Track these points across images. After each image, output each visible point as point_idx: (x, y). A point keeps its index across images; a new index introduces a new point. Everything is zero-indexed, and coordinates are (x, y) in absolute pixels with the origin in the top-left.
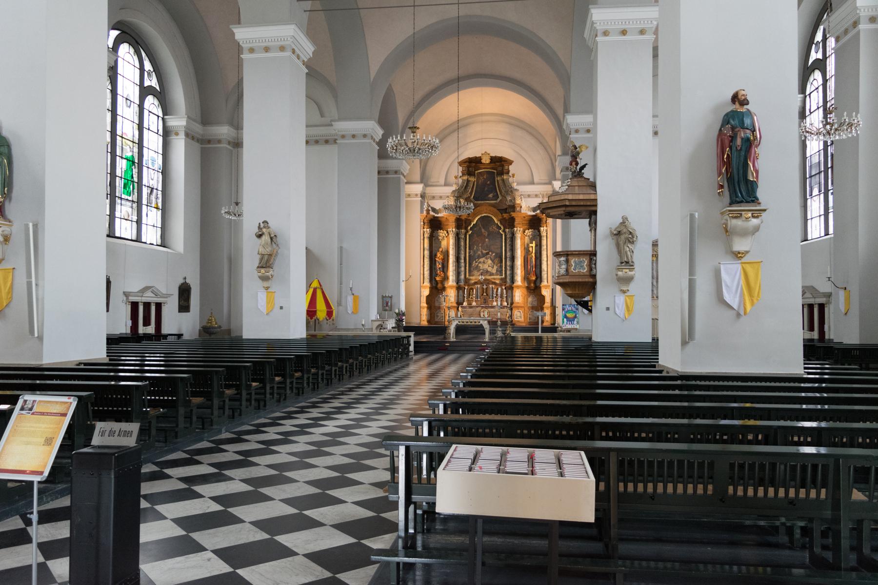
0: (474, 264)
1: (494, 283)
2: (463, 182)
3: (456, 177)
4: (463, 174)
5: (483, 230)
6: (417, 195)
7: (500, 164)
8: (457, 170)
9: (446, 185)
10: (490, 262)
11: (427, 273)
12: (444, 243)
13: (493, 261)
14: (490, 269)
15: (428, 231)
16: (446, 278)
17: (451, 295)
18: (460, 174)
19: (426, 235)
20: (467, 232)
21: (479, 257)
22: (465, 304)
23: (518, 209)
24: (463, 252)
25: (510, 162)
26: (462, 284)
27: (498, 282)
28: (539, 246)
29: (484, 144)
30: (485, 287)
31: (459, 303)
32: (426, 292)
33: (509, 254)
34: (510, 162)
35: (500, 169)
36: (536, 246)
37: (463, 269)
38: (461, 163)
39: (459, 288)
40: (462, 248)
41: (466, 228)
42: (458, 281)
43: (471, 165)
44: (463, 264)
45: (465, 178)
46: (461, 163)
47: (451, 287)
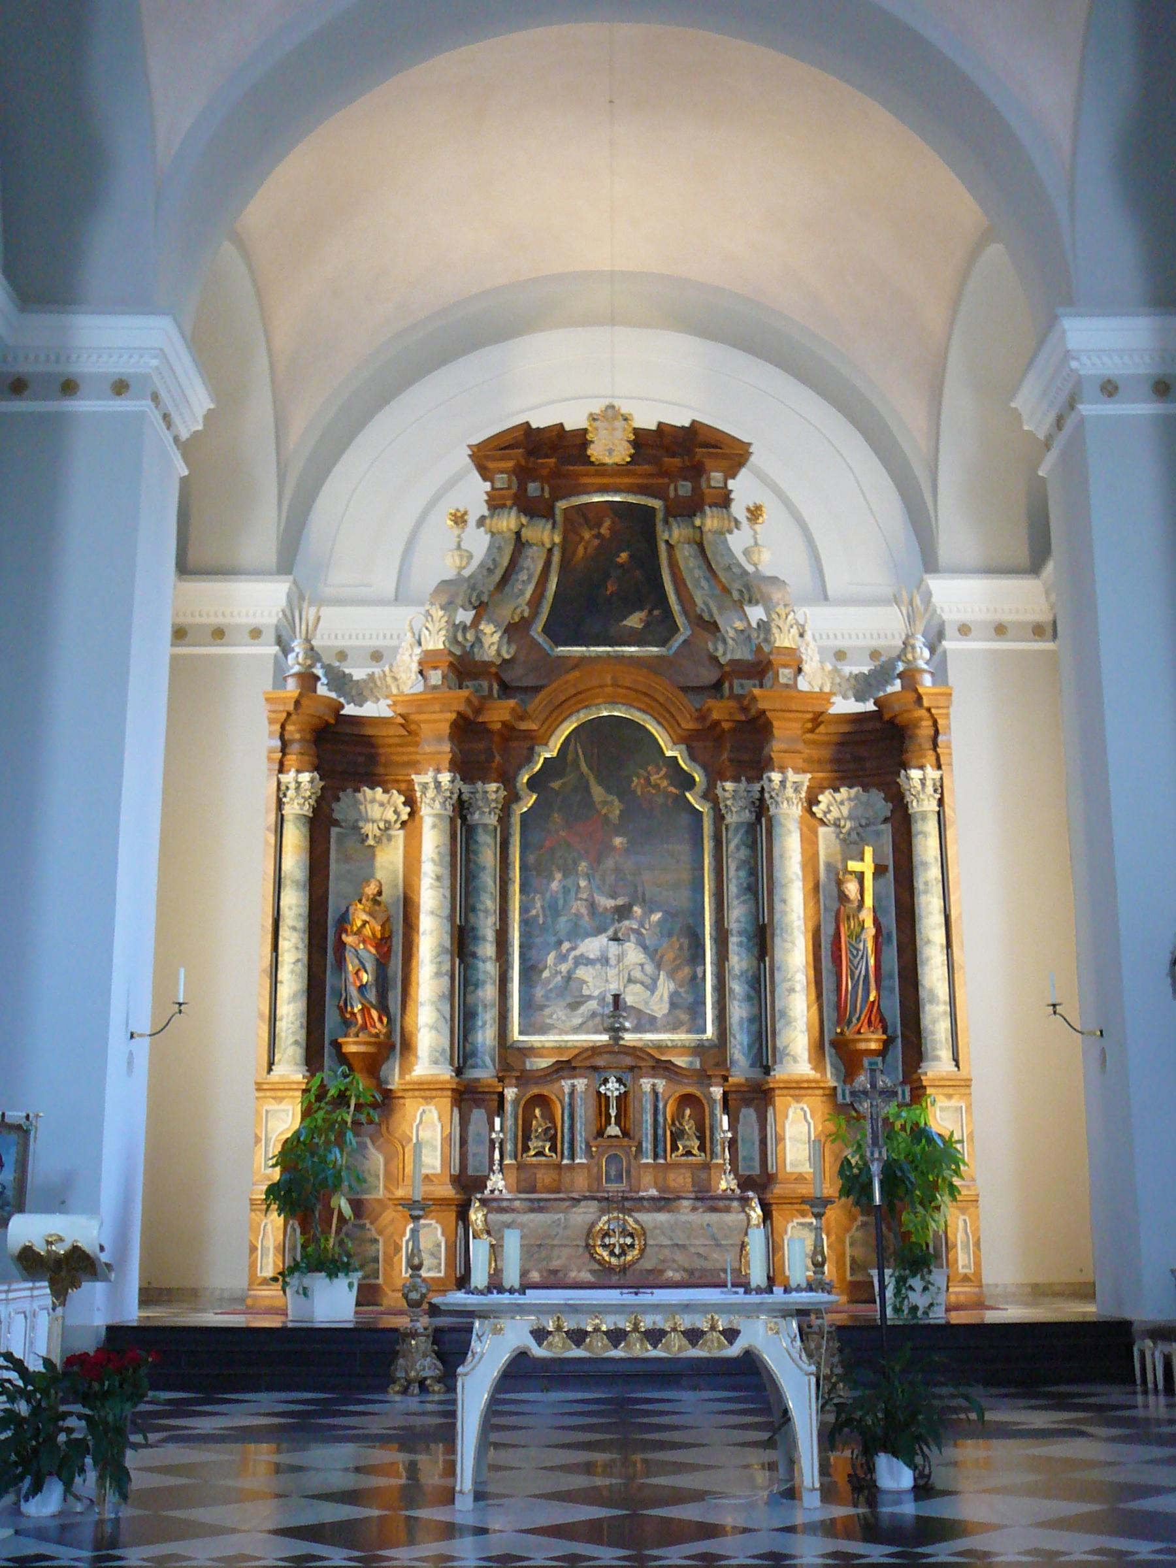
2: (494, 548)
3: (459, 519)
4: (495, 504)
5: (597, 792)
6: (256, 633)
7: (686, 462)
9: (399, 598)
10: (633, 954)
11: (291, 1012)
12: (389, 861)
13: (651, 953)
14: (633, 996)
15: (302, 782)
16: (395, 1044)
17: (427, 1132)
18: (478, 507)
19: (296, 808)
20: (513, 797)
21: (577, 933)
22: (497, 1182)
23: (785, 675)
24: (488, 903)
25: (735, 455)
27: (681, 1061)
28: (901, 872)
29: (609, 381)
30: (612, 1088)
31: (469, 1183)
32: (285, 1119)
33: (737, 914)
34: (735, 455)
35: (684, 488)
36: (879, 870)
37: (489, 992)
38: (485, 457)
39: (467, 1096)
40: (488, 881)
41: (507, 779)
42: (462, 1054)
43: (534, 464)
44: (489, 969)
45: (509, 522)
46: (485, 457)
47: (426, 1089)
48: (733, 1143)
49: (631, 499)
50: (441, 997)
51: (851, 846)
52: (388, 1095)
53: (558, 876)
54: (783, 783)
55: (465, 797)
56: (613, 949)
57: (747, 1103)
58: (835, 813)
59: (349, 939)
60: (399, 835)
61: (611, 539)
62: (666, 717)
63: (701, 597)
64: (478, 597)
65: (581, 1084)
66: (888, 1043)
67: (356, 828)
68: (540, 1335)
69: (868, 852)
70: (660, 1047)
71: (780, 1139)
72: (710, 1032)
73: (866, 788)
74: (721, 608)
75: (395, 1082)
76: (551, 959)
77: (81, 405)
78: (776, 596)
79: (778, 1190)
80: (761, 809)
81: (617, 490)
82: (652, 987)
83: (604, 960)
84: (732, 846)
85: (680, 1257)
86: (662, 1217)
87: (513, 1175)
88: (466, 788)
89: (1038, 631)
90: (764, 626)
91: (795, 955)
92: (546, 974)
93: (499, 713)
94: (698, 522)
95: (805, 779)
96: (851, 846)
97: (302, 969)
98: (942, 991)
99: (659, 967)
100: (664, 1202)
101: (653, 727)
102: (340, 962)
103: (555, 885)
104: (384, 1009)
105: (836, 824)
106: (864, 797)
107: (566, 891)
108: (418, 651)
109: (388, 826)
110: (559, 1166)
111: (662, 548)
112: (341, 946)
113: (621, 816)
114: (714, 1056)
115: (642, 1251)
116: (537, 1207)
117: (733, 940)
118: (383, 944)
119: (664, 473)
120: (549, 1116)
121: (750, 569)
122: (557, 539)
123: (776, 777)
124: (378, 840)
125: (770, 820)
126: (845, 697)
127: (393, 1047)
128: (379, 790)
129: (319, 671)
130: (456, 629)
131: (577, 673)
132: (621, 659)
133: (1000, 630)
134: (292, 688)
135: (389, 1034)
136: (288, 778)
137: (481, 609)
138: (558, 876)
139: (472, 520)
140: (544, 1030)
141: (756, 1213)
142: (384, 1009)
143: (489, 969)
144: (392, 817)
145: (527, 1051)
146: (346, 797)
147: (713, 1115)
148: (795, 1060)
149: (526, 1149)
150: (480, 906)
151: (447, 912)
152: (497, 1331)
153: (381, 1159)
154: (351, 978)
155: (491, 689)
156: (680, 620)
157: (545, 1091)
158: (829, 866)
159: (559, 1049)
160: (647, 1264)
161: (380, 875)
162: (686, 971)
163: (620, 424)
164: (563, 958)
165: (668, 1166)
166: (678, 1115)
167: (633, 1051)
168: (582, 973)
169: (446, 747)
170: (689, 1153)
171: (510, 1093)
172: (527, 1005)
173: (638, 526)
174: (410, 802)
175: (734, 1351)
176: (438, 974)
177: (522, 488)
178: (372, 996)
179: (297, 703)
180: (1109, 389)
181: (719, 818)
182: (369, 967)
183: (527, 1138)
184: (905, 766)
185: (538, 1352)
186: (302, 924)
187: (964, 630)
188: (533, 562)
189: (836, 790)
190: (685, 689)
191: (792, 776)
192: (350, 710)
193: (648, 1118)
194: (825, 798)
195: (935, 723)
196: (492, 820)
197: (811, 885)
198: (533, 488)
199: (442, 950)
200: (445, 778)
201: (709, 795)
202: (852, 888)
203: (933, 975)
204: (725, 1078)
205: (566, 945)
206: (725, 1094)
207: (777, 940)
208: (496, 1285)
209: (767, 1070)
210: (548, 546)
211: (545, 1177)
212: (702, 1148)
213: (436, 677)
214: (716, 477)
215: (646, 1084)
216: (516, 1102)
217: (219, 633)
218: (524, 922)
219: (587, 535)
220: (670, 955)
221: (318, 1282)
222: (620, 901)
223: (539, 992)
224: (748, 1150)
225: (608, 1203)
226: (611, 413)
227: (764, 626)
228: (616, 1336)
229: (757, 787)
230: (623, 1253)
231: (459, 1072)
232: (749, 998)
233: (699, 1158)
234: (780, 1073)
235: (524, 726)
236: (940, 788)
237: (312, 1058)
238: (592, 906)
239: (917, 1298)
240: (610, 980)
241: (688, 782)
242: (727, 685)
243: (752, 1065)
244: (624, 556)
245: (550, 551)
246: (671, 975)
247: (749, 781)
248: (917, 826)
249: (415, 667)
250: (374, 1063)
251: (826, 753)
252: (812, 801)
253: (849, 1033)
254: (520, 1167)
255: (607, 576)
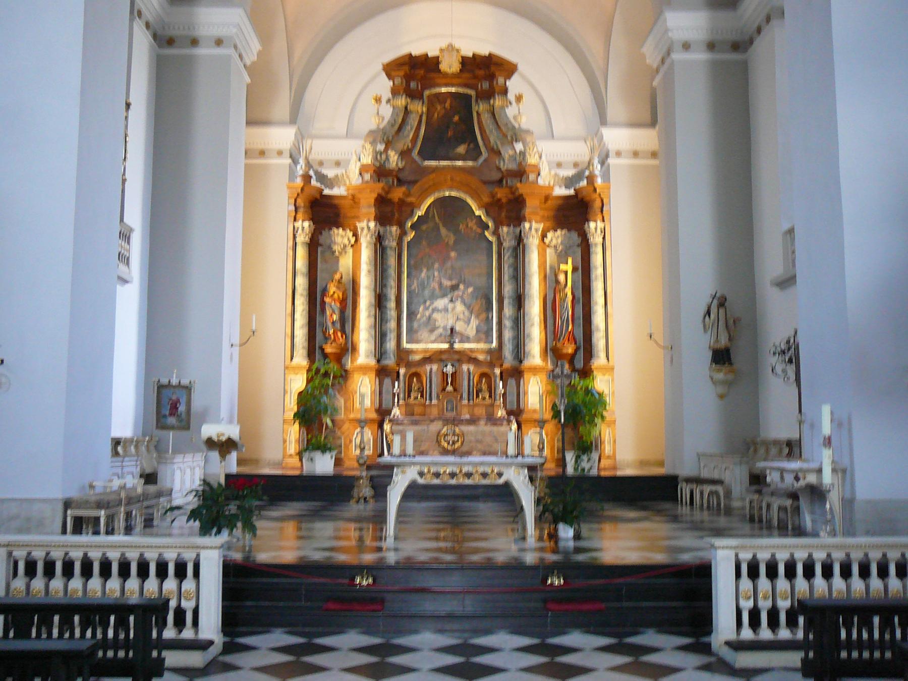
0: (422, 313)
1: (474, 361)
3: (378, 100)
4: (395, 92)
5: (443, 231)
6: (280, 153)
7: (486, 73)
8: (385, 86)
9: (349, 135)
10: (460, 307)
11: (301, 333)
12: (345, 263)
13: (469, 307)
14: (459, 327)
15: (305, 226)
16: (349, 348)
17: (364, 388)
18: (386, 94)
19: (302, 238)
20: (403, 233)
22: (396, 412)
23: (532, 177)
24: (392, 283)
25: (509, 69)
26: (390, 361)
27: (481, 357)
30: (449, 369)
31: (383, 413)
32: (299, 383)
33: (508, 289)
34: (509, 69)
35: (486, 85)
36: (575, 269)
37: (392, 324)
38: (390, 69)
39: (382, 372)
40: (392, 272)
41: (401, 225)
42: (380, 353)
43: (414, 73)
45: (401, 101)
46: (390, 69)
47: (364, 369)
48: (504, 395)
49: (461, 90)
50: (370, 327)
51: (562, 257)
52: (346, 371)
53: (425, 270)
54: (530, 228)
55: (381, 233)
56: (450, 306)
57: (512, 376)
58: (554, 242)
59: (327, 300)
60: (350, 251)
61: (451, 107)
62: (476, 195)
63: (493, 139)
64: (388, 138)
65: (435, 367)
66: (576, 350)
67: (330, 248)
68: (421, 474)
69: (570, 261)
70: (471, 350)
71: (526, 393)
72: (494, 344)
73: (569, 230)
74: (502, 144)
75: (349, 366)
76: (421, 309)
77: (201, 51)
78: (529, 139)
79: (524, 416)
80: (520, 240)
81: (453, 85)
82: (468, 322)
83: (446, 310)
84: (506, 258)
85: (479, 446)
86: (471, 428)
87: (403, 409)
88: (382, 230)
89: (654, 155)
90: (523, 154)
91: (534, 309)
92: (419, 316)
93: (398, 194)
94: (492, 102)
95: (541, 226)
96: (562, 257)
97: (306, 314)
98: (602, 326)
99: (471, 313)
100: (473, 421)
101: (470, 201)
102: (323, 310)
103: (423, 275)
104: (343, 331)
105: (555, 247)
106: (568, 235)
107: (428, 278)
108: (359, 164)
109: (345, 246)
110: (424, 405)
111: (475, 115)
112: (323, 303)
113: (455, 242)
114: (496, 355)
115: (462, 443)
116: (415, 423)
117: (506, 302)
118: (343, 302)
119: (475, 77)
120: (420, 381)
121: (517, 126)
122: (425, 109)
123: (527, 225)
124: (340, 253)
125: (524, 246)
126: (560, 187)
127: (348, 350)
128: (341, 230)
129: (311, 173)
130: (376, 154)
131: (434, 175)
132: (455, 168)
133: (636, 154)
134: (299, 182)
135: (346, 344)
136: (299, 224)
137: (388, 144)
138: (425, 270)
139: (384, 100)
140: (418, 342)
141: (514, 426)
142: (343, 331)
143: (392, 313)
144: (346, 241)
145: (409, 352)
146: (325, 233)
147: (495, 381)
148: (534, 357)
149: (409, 396)
150: (388, 284)
151: (373, 286)
152: (403, 472)
153: (342, 401)
154: (328, 317)
155: (393, 182)
156: (483, 149)
157: (419, 370)
158: (551, 268)
159: (425, 351)
160: (465, 449)
161: (341, 269)
162: (484, 316)
163: (455, 53)
164: (427, 309)
165: (474, 406)
166: (480, 381)
167: (459, 352)
168: (435, 315)
169: (373, 210)
170: (484, 399)
171: (402, 371)
172: (410, 330)
173: (463, 103)
174: (355, 235)
175: (501, 481)
176: (369, 316)
177: (408, 84)
178: (338, 326)
179: (302, 189)
180: (686, 46)
181: (500, 244)
182: (337, 311)
183: (410, 391)
184: (588, 220)
185: (421, 481)
186: (306, 293)
187: (618, 154)
188: (413, 121)
189: (556, 231)
190: (485, 183)
191: (534, 225)
192: (327, 192)
193: (466, 383)
194: (550, 235)
195: (602, 201)
196: (394, 244)
197: (543, 275)
198: (413, 85)
199: (370, 305)
200: (372, 224)
201: (496, 233)
202: (562, 278)
203: (598, 319)
204: (501, 366)
205: (428, 303)
206: (501, 373)
207: (526, 302)
208: (403, 454)
209: (521, 362)
210: (420, 111)
211: (417, 410)
212: (490, 396)
213: (367, 177)
214: (501, 80)
215: (465, 367)
216: (405, 376)
217: (262, 153)
218: (409, 292)
219: (439, 108)
220: (476, 308)
221: (318, 455)
222: (454, 282)
223: (415, 325)
224: (511, 398)
225: (446, 422)
226: (451, 48)
227: (523, 154)
228: (453, 475)
229: (518, 230)
230: (454, 443)
231: (378, 361)
232: (513, 328)
233: (488, 401)
234: (527, 363)
235: (410, 200)
236: (604, 231)
237: (311, 354)
238: (440, 284)
239: (585, 464)
240: (448, 320)
241: (487, 227)
242: (504, 182)
243: (514, 358)
244: (456, 118)
245: (421, 116)
246: (477, 316)
247: (514, 226)
248: (592, 250)
249: (357, 172)
250: (339, 357)
251: (551, 213)
252: (544, 236)
253: (559, 345)
254: (407, 405)
255: (448, 127)
